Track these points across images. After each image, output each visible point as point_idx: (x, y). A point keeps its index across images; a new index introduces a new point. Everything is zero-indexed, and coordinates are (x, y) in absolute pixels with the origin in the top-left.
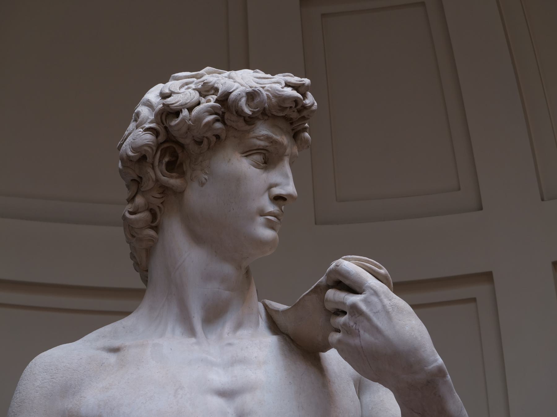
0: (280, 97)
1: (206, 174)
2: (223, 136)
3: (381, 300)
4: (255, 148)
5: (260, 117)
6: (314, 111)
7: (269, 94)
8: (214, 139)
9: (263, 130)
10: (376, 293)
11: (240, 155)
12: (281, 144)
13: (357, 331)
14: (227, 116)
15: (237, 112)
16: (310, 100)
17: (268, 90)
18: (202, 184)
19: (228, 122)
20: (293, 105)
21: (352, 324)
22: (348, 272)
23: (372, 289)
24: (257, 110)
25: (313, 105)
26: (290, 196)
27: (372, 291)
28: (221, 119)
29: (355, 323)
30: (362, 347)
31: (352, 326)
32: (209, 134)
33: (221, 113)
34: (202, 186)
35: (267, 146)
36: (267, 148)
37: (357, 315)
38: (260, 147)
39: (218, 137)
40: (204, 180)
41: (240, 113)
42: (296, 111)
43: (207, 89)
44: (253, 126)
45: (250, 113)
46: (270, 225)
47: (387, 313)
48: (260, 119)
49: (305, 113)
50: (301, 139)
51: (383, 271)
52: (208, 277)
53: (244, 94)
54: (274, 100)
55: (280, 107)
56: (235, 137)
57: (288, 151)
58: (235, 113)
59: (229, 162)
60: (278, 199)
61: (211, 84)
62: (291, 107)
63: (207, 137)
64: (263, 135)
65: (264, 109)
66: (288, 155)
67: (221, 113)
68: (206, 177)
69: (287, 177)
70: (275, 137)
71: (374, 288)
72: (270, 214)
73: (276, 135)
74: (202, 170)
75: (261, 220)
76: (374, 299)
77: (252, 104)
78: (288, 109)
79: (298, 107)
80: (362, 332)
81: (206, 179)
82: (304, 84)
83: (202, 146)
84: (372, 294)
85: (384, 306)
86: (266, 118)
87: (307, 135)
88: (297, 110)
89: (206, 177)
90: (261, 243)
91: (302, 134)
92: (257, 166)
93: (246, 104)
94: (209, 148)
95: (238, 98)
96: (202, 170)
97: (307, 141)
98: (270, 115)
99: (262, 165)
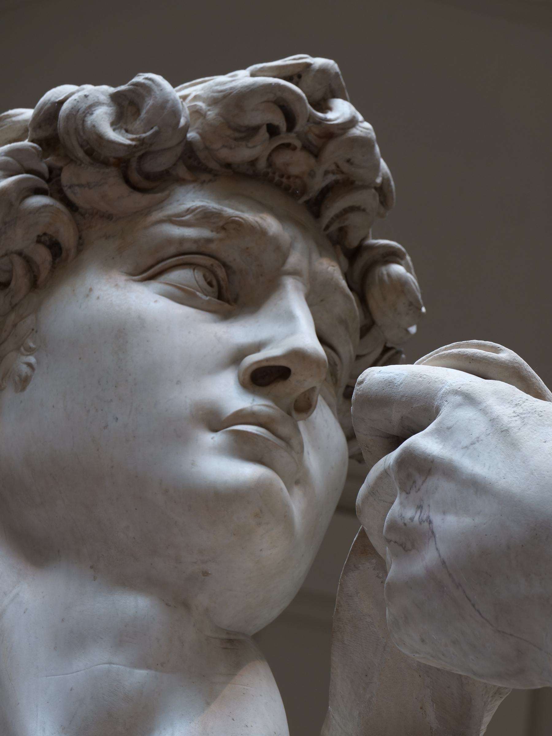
0: (225, 97)
1: (30, 351)
2: (67, 235)
3: (484, 411)
4: (172, 250)
5: (182, 171)
6: (363, 143)
7: (201, 104)
8: (42, 256)
9: (191, 199)
10: (469, 399)
11: (124, 277)
12: (260, 233)
13: (426, 524)
14: (66, 177)
15: (89, 153)
16: (341, 110)
17: (196, 98)
18: (23, 383)
19: (78, 197)
20: (279, 121)
21: (410, 513)
22: (390, 383)
23: (456, 392)
24: (148, 134)
25: (352, 123)
26: (299, 355)
27: (458, 399)
28: (51, 183)
29: (420, 507)
30: (443, 563)
31: (412, 519)
32: (20, 239)
33: (43, 167)
34: (23, 389)
35: (209, 241)
36: (213, 247)
37: (419, 482)
38: (187, 247)
39: (55, 247)
40: (25, 369)
41: (95, 149)
42: (298, 144)
43: (13, 135)
44: (159, 195)
45: (128, 142)
46: (245, 449)
47: (503, 432)
48: (181, 181)
49: (333, 153)
50: (381, 280)
51: (507, 354)
52: (72, 640)
53: (103, 98)
54: (211, 114)
55: (237, 129)
56: (107, 237)
57: (295, 259)
58: (80, 154)
59: (87, 296)
60: (264, 377)
61: (20, 118)
62: (273, 130)
63: (20, 254)
64: (189, 211)
65: (189, 145)
66: (295, 273)
67: (43, 167)
68: (32, 359)
69: (290, 317)
70: (229, 211)
71: (464, 388)
72: (242, 417)
73: (242, 211)
74: (18, 349)
75: (212, 439)
76: (466, 414)
77: (137, 124)
78: (264, 134)
79: (298, 128)
80: (437, 520)
81: (30, 365)
82: (308, 65)
83: (13, 283)
84: (460, 405)
85: (493, 421)
86: (205, 177)
87: (398, 269)
88: (298, 136)
89: (32, 359)
90: (223, 500)
91: (384, 270)
92: (185, 297)
93: (116, 124)
94: (34, 284)
95: (83, 106)
96: (18, 349)
97: (400, 285)
98: (213, 165)
99: (204, 297)
